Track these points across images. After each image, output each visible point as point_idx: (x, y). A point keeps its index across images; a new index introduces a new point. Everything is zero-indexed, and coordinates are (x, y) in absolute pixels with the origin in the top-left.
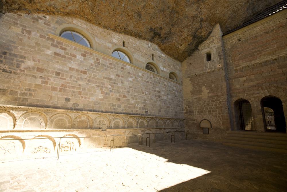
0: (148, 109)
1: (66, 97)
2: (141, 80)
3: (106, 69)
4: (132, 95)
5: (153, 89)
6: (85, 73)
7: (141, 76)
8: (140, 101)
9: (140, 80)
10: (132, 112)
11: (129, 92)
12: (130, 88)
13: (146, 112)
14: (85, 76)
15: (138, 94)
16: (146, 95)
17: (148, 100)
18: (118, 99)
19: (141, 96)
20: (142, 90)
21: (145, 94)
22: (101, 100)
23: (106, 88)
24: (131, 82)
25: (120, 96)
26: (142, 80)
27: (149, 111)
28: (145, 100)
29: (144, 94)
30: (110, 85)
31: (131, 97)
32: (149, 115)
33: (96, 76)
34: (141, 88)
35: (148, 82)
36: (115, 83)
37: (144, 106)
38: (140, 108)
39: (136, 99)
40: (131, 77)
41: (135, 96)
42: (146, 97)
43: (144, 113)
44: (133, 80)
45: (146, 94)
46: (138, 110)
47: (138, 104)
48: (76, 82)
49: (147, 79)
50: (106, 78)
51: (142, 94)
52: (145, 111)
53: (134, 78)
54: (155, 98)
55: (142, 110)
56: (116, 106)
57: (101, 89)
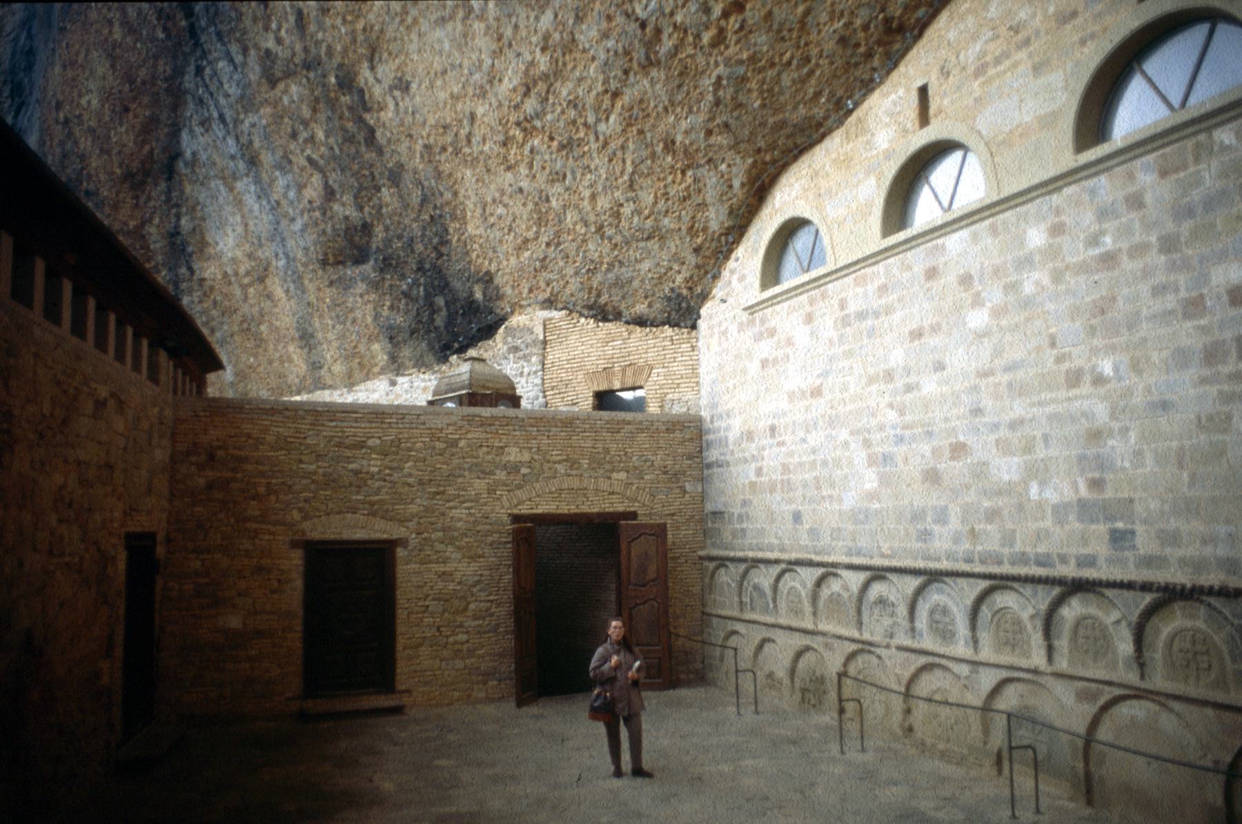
0: (1138, 508)
1: (793, 507)
2: (1046, 281)
3: (871, 333)
4: (995, 427)
5: (1170, 301)
6: (817, 392)
7: (1040, 251)
8: (1053, 452)
9: (1037, 283)
10: (1011, 546)
11: (977, 411)
12: (983, 383)
13: (1119, 538)
14: (820, 406)
15: (1040, 404)
16: (1102, 391)
17: (1125, 431)
18: (932, 477)
19: (1059, 409)
20: (1059, 360)
21: (1087, 379)
22: (872, 496)
23: (881, 428)
24: (981, 335)
25: (936, 452)
26: (1057, 277)
27: (1139, 529)
28: (1096, 436)
29: (1086, 388)
30: (891, 406)
31: (992, 438)
32: (1148, 562)
33: (845, 388)
34: (1053, 345)
35: (1109, 260)
36: (909, 388)
37: (1096, 484)
38: (1060, 512)
39: (1028, 449)
40: (977, 302)
41: (1014, 425)
42: (1101, 411)
43: (1100, 548)
44: (997, 313)
45: (1099, 380)
46: (1048, 523)
47: (1043, 484)
48: (804, 440)
49: (1094, 241)
50: (871, 380)
51: (1063, 394)
52: (1102, 528)
53: (995, 295)
54: (1204, 381)
55: (1081, 521)
56: (929, 519)
57: (867, 443)
